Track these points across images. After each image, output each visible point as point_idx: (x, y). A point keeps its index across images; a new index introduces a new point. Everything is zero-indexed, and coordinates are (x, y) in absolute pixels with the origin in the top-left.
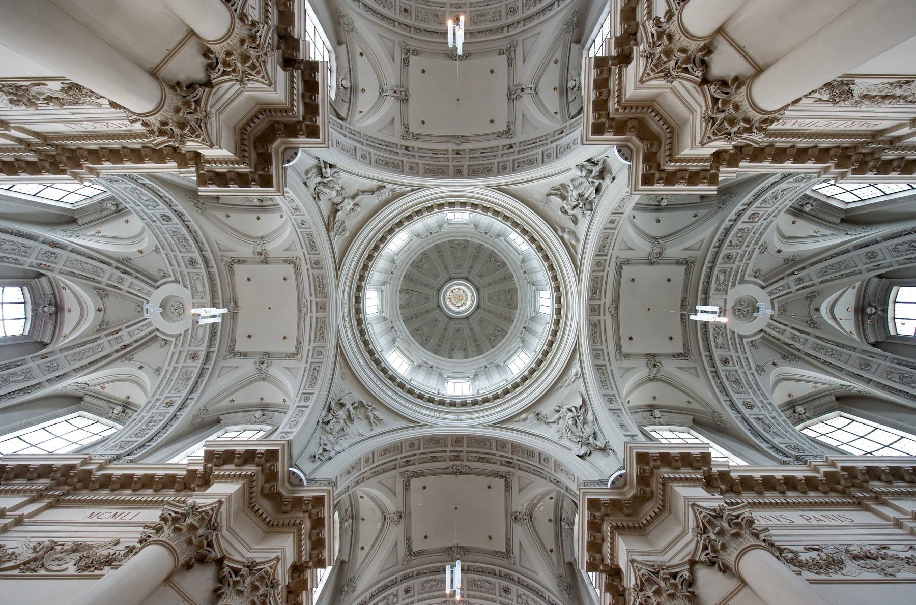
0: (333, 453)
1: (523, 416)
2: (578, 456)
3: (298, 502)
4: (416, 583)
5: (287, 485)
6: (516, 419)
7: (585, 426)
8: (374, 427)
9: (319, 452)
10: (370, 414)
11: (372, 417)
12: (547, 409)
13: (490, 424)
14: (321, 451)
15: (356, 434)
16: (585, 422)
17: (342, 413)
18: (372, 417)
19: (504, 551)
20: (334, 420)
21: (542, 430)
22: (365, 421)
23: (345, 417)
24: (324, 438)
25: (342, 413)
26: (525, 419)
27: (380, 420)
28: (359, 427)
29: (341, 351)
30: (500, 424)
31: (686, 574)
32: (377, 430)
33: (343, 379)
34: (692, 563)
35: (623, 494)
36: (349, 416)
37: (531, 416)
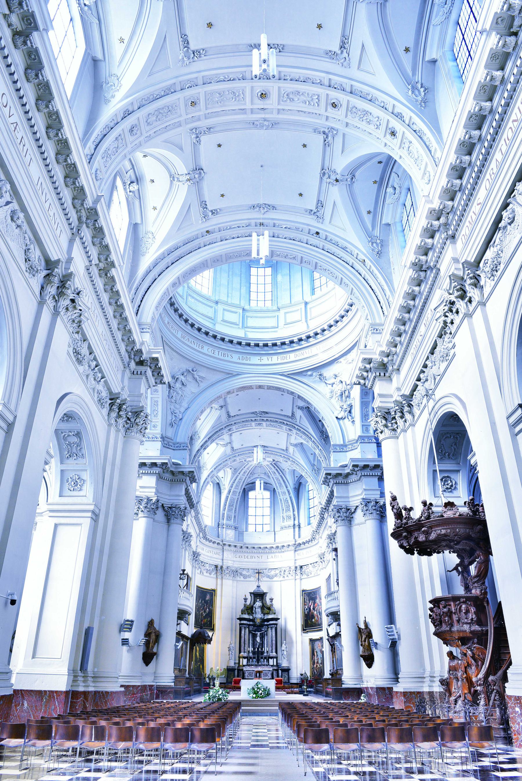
0: (181, 417)
1: (309, 373)
2: (337, 418)
3: (182, 473)
4: (234, 427)
5: (173, 466)
6: (304, 374)
7: (348, 399)
8: (201, 384)
9: (173, 420)
10: (196, 376)
11: (198, 377)
12: (328, 372)
13: (285, 374)
14: (174, 419)
15: (190, 393)
16: (348, 397)
17: (178, 385)
18: (198, 377)
19: (290, 415)
20: (175, 393)
21: (321, 387)
22: (194, 381)
23: (180, 386)
24: (172, 407)
25: (178, 385)
26: (311, 375)
27: (203, 378)
28: (192, 388)
29: (167, 344)
30: (292, 375)
31: (353, 510)
32: (203, 385)
33: (172, 360)
34: (357, 507)
35: (344, 470)
36: (183, 384)
37: (314, 374)
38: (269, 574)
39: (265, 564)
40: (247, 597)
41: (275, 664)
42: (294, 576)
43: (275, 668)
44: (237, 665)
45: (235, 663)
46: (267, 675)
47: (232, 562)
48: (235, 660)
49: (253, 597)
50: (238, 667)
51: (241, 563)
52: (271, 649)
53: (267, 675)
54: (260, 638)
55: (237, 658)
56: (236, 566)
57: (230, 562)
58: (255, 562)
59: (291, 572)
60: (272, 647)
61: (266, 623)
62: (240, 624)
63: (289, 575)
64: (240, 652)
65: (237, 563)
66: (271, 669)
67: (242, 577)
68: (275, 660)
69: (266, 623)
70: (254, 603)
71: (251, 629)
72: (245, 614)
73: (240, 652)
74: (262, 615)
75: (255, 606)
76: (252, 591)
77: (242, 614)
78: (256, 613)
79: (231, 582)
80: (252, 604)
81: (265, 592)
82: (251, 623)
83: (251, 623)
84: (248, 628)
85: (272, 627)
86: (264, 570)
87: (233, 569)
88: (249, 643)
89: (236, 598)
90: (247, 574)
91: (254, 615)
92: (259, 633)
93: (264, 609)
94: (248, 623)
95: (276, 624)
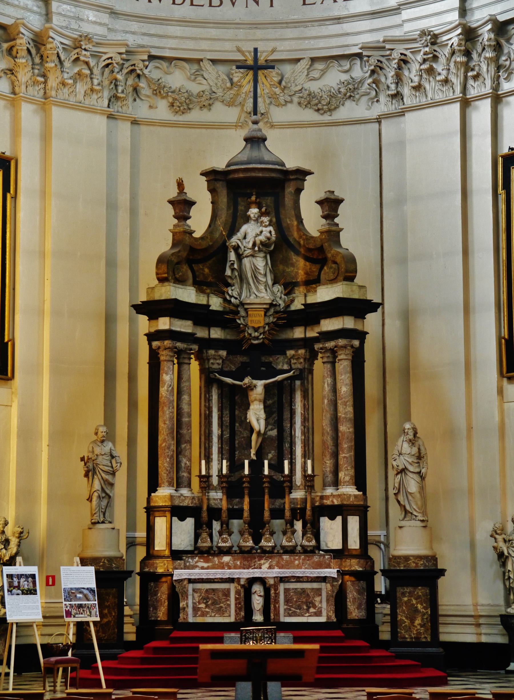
38: (314, 87)
39: (290, 33)
40: (191, 194)
41: (354, 543)
42: (457, 82)
43: (355, 565)
44: (141, 552)
45: (131, 544)
46: (310, 604)
47: (105, 18)
48: (131, 526)
49: (223, 199)
50: (143, 562)
51: (154, 29)
52: (329, 463)
53: (310, 604)
54: (268, 410)
55: (142, 517)
56: (132, 40)
57: (91, 15)
58: (238, 25)
59: (439, 67)
60: (335, 455)
61: (298, 333)
62: (151, 337)
63: (430, 85)
64: (153, 486)
65: (134, 26)
66: (332, 572)
67: (163, 105)
68: (354, 522)
69: (298, 333)
70: (233, 230)
71: (215, 365)
72: (180, 281)
73: (153, 486)
74: (278, 288)
75: (234, 240)
76: (221, 165)
77: (162, 280)
78: (242, 278)
79: (101, 121)
80: (221, 229)
81: (290, 164)
82: (216, 333)
83: (216, 333)
84: (199, 358)
85: (333, 352)
86: (287, 69)
87: (111, 52)
88: (207, 436)
89: (133, 212)
90: (195, 88)
91: (233, 291)
92: (260, 384)
93: (286, 262)
94: (201, 333)
95: (361, 335)
